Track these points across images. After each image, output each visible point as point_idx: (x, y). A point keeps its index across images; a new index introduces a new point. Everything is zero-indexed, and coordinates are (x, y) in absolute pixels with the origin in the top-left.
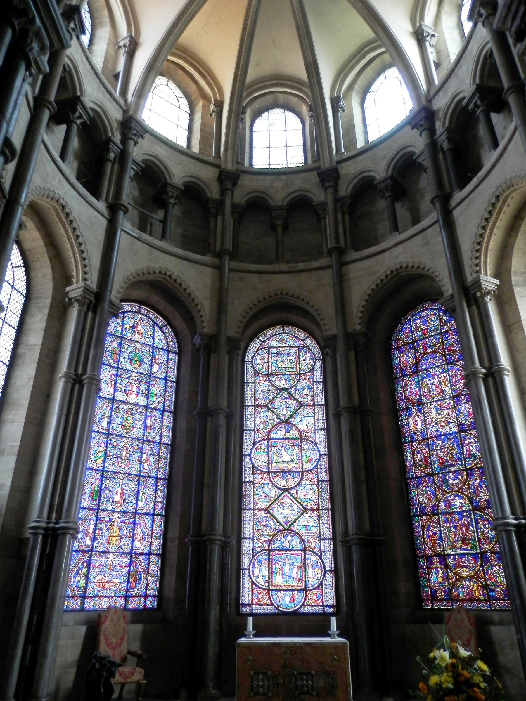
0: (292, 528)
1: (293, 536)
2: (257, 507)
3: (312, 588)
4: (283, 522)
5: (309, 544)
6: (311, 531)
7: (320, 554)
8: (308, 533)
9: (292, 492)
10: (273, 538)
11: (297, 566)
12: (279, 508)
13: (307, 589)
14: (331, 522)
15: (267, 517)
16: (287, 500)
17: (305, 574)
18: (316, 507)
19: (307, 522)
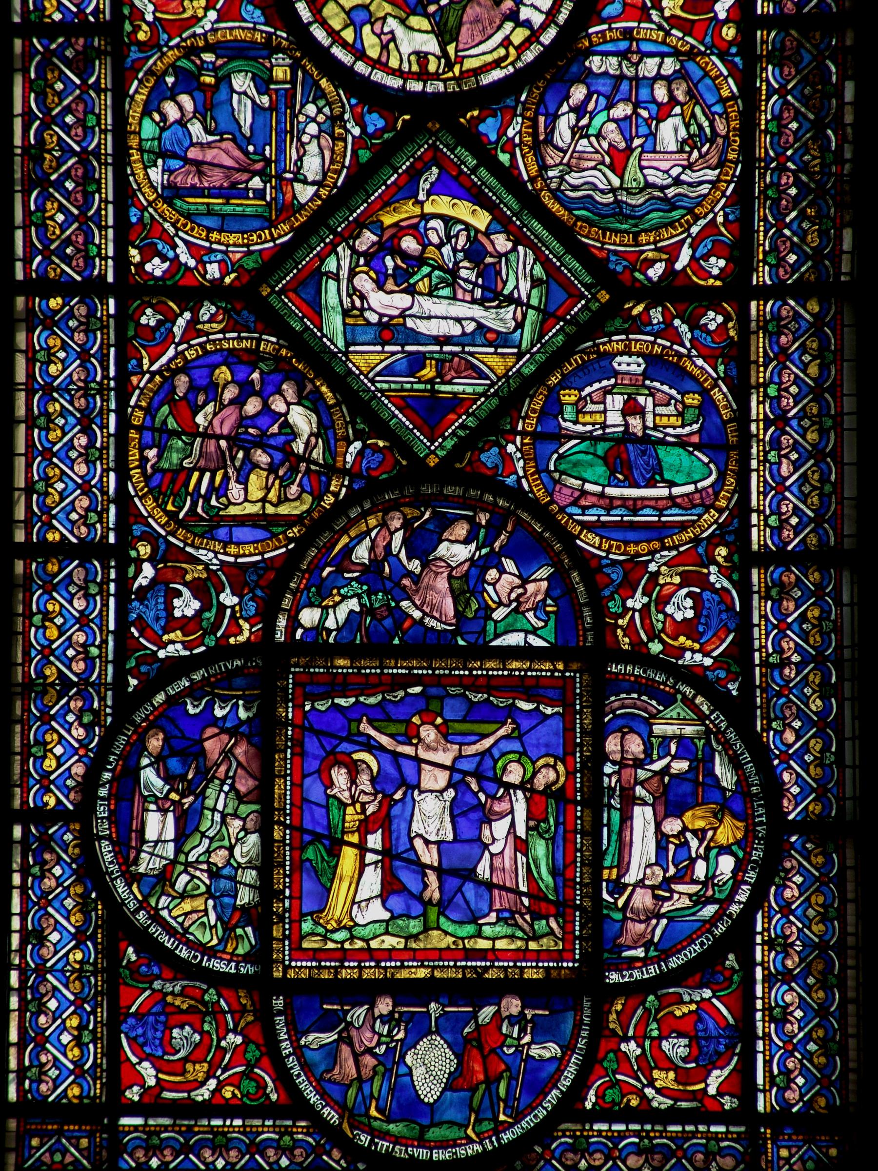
0: (490, 457)
1: (494, 530)
2: (156, 267)
3: (653, 970)
4: (406, 404)
5: (637, 602)
6: (663, 492)
7: (733, 688)
8: (634, 506)
9: (489, 128)
10: (303, 543)
11: (525, 785)
12: (364, 283)
13: (614, 977)
14: (848, 404)
15: (252, 358)
16: (442, 205)
17: (599, 854)
18: (716, 265)
19: (631, 409)
